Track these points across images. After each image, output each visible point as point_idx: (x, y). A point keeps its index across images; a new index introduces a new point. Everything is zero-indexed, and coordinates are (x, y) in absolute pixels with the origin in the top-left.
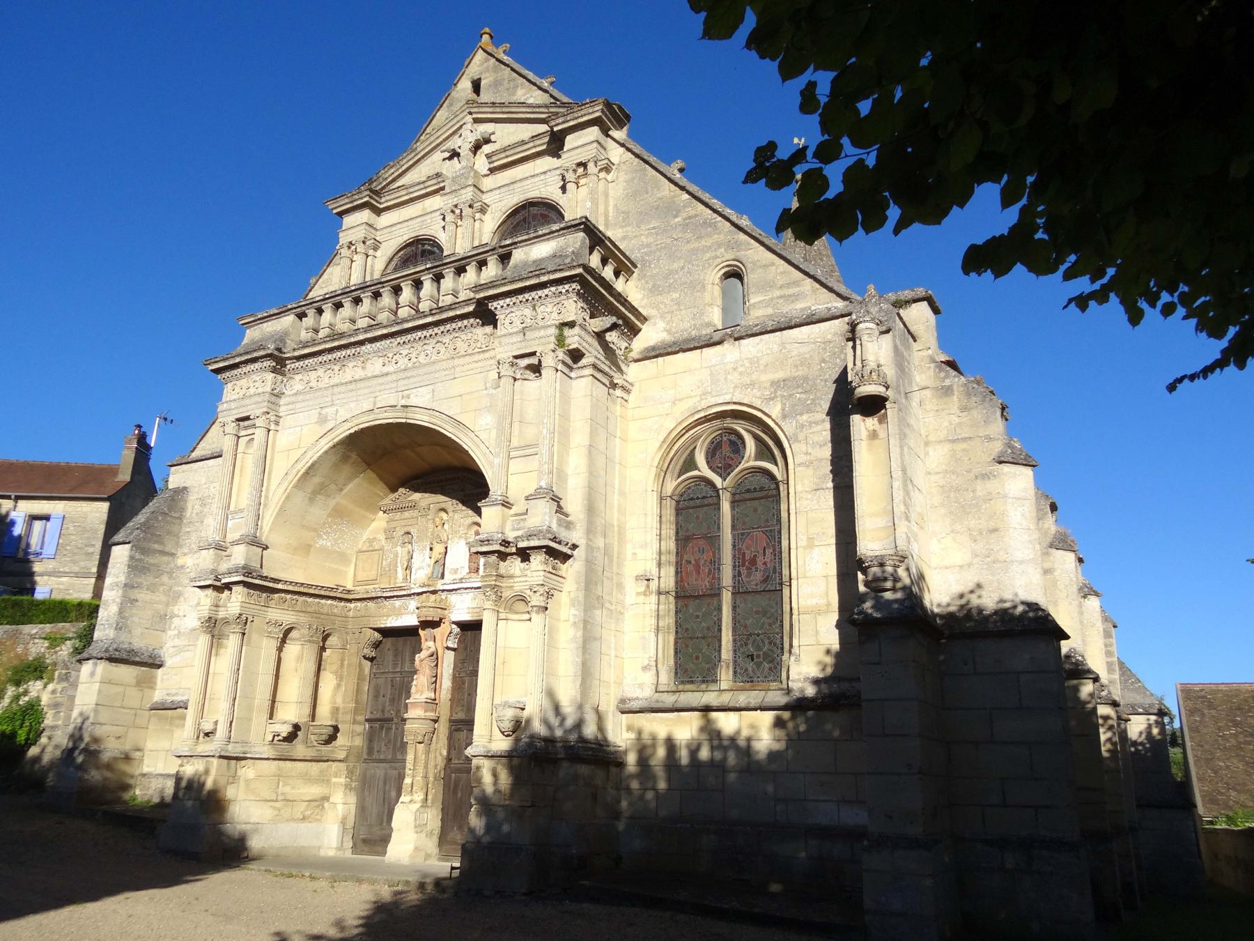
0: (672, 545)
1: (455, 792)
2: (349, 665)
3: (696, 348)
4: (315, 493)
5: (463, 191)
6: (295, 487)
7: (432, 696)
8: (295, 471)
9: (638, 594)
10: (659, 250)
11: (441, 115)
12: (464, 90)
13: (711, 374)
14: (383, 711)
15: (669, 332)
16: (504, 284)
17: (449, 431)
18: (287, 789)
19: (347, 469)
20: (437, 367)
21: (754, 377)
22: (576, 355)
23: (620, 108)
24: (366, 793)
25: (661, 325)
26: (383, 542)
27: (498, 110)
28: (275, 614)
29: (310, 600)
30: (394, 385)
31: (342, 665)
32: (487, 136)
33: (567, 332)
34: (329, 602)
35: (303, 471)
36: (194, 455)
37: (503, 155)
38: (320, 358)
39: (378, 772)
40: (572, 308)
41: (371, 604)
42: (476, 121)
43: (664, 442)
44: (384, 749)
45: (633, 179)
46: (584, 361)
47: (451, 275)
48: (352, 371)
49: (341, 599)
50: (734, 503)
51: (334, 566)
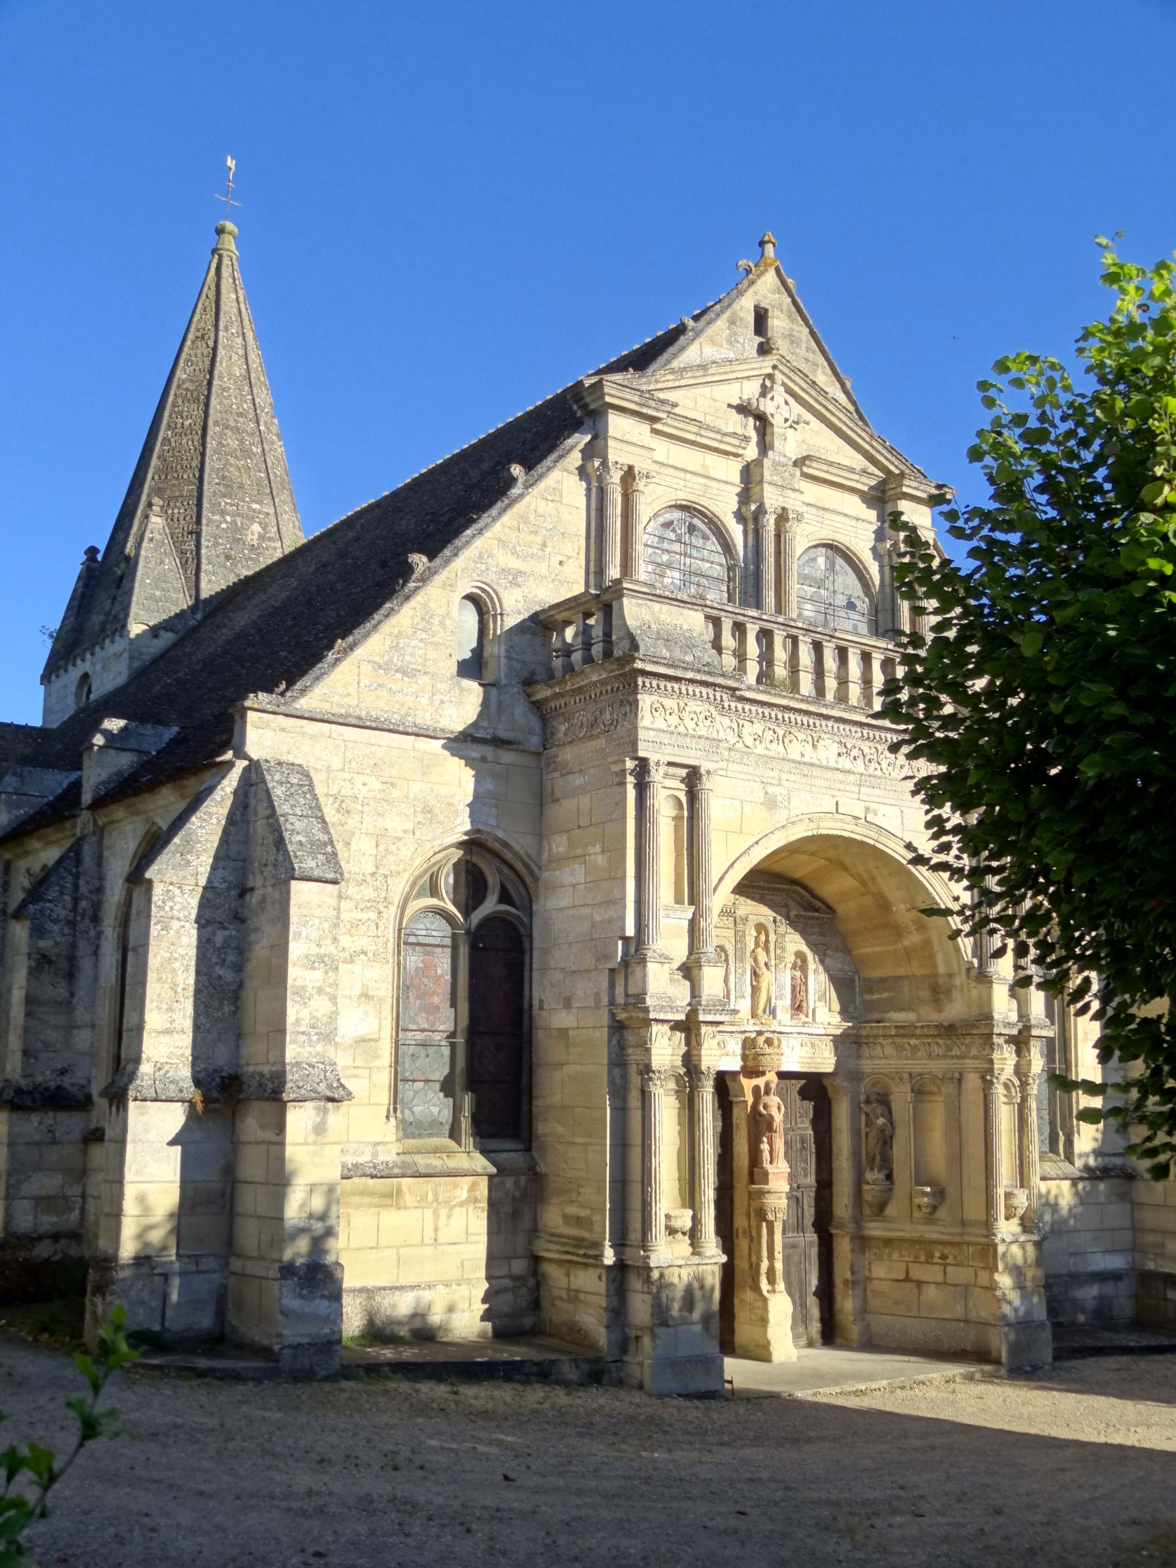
27: (813, 393)
36: (304, 703)
37: (825, 468)
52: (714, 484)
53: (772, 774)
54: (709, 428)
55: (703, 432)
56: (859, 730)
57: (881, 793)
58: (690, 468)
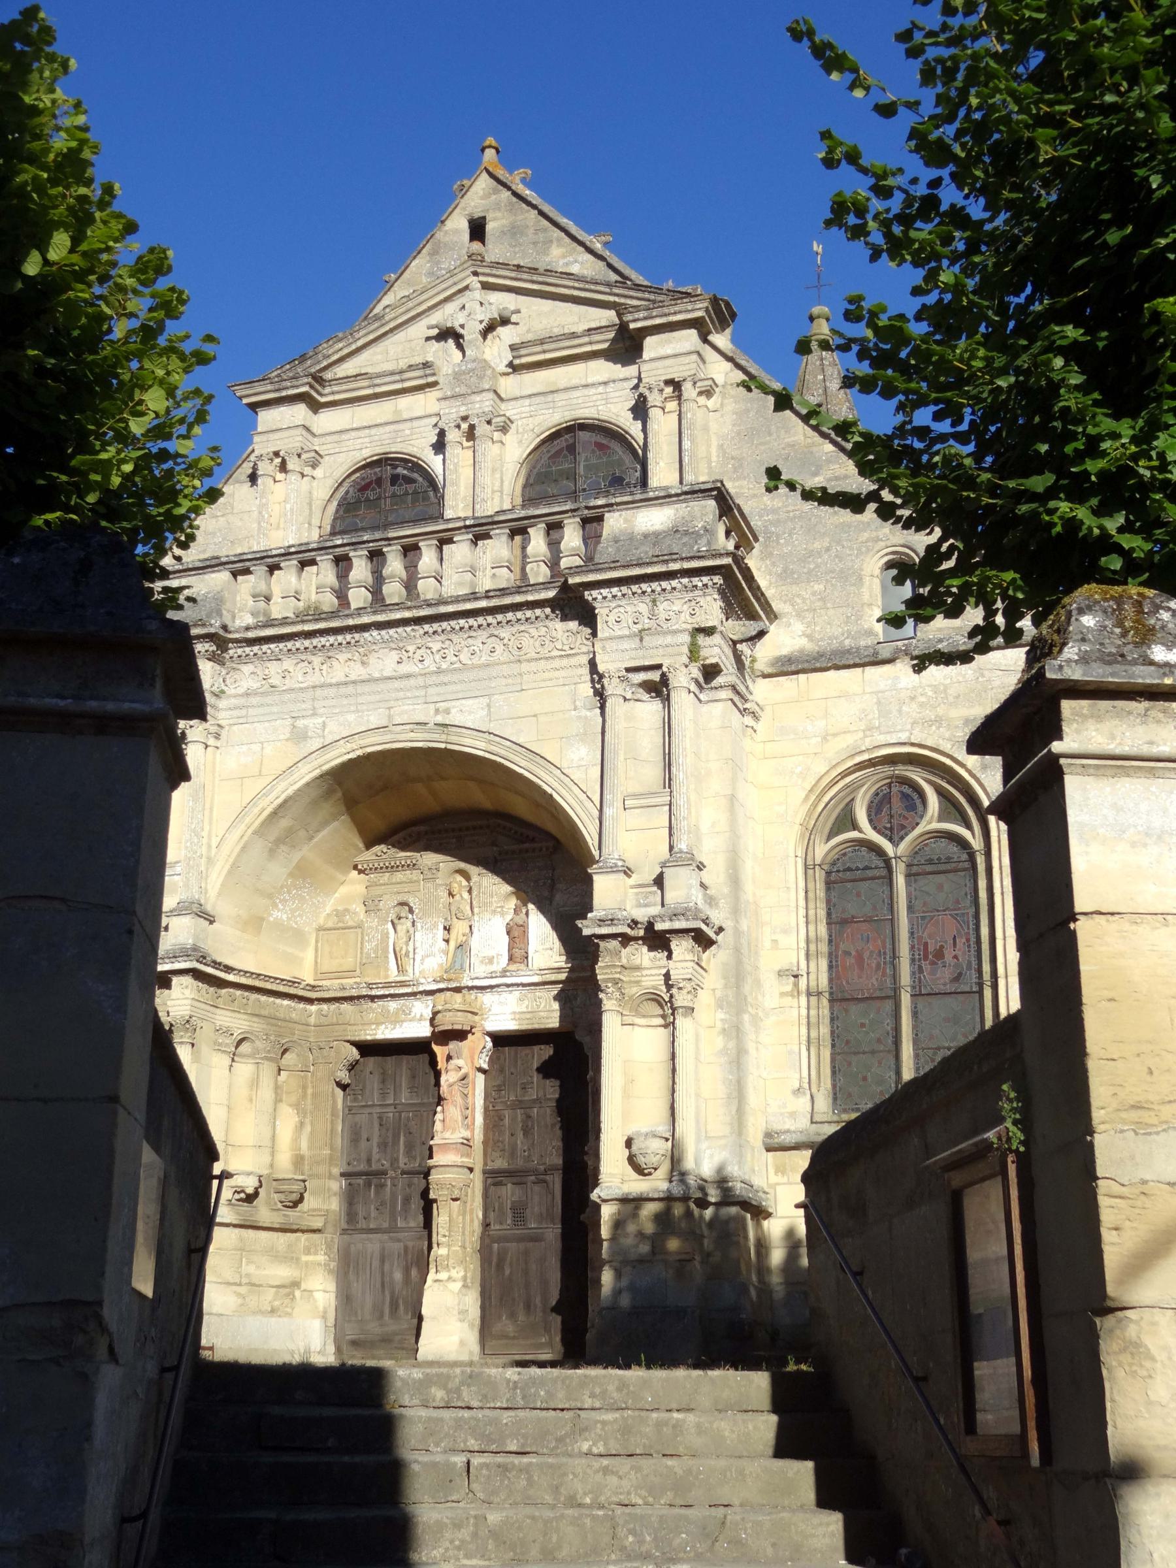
0: (823, 930)
1: (500, 1267)
2: (314, 1095)
3: (855, 666)
4: (279, 841)
5: (477, 398)
6: (255, 833)
7: (467, 1134)
8: (256, 810)
9: (783, 994)
10: (792, 519)
11: (419, 267)
12: (457, 231)
13: (879, 703)
14: (369, 1161)
15: (810, 637)
16: (615, 568)
17: (520, 765)
18: (251, 1269)
19: (327, 808)
20: (494, 672)
21: (940, 711)
22: (711, 672)
23: (727, 304)
24: (352, 1276)
25: (798, 627)
26: (362, 916)
27: (525, 276)
28: (224, 1018)
29: (264, 998)
30: (423, 693)
31: (304, 1096)
32: (506, 314)
33: (702, 640)
34: (286, 1002)
35: (269, 810)
37: (538, 349)
38: (290, 645)
39: (369, 1246)
40: (711, 609)
41: (345, 1006)
42: (486, 286)
43: (811, 791)
44: (373, 1214)
45: (747, 411)
46: (720, 680)
47: (504, 538)
48: (344, 666)
49: (301, 999)
50: (908, 876)
51: (290, 950)
52: (408, 424)
53: (303, 706)
54: (379, 376)
55: (378, 381)
56: (416, 628)
57: (458, 687)
58: (379, 421)
